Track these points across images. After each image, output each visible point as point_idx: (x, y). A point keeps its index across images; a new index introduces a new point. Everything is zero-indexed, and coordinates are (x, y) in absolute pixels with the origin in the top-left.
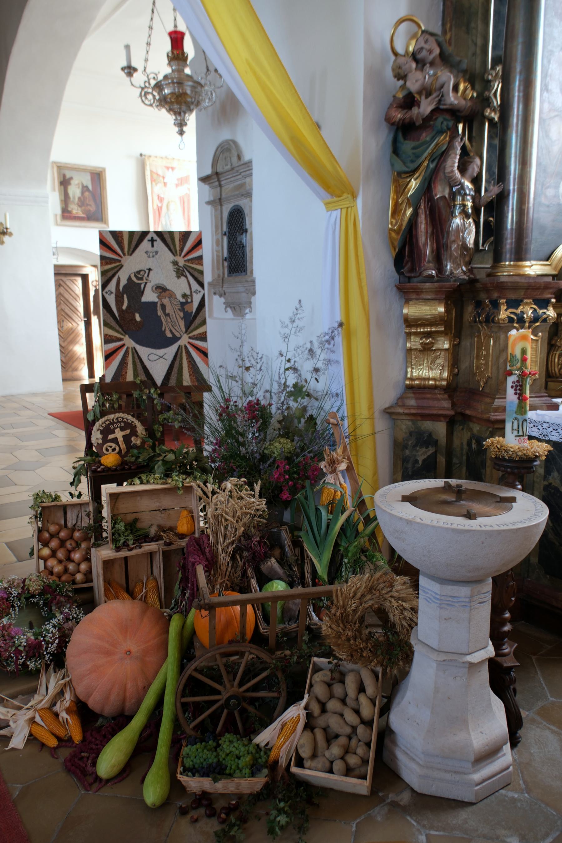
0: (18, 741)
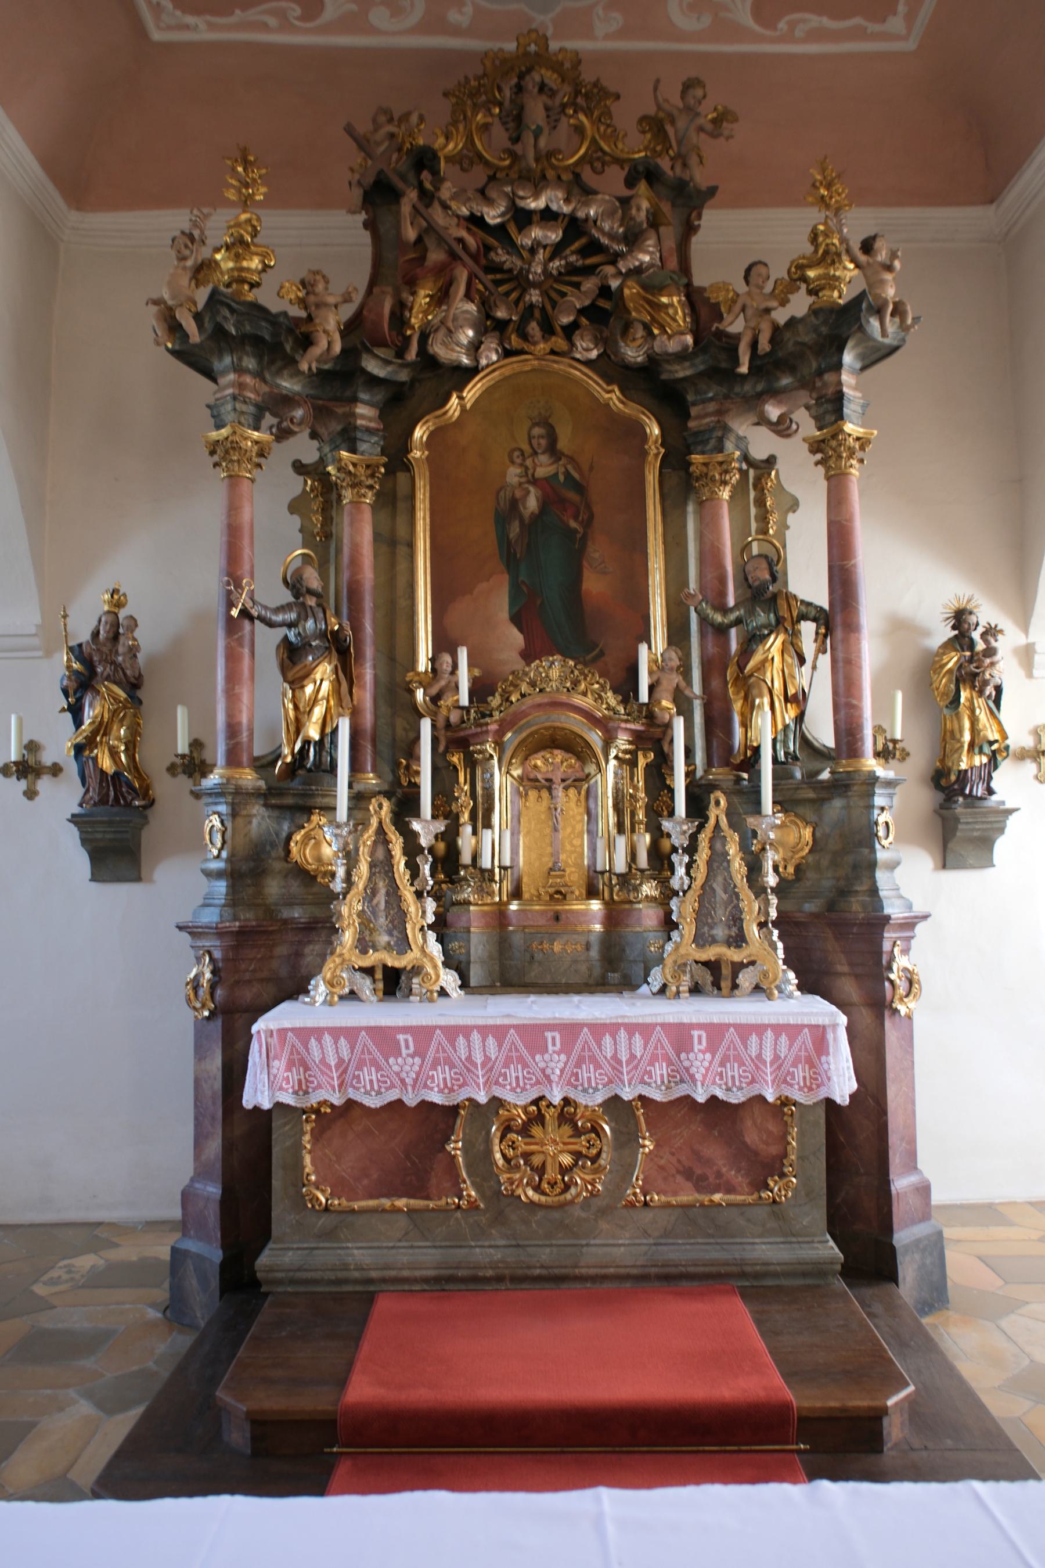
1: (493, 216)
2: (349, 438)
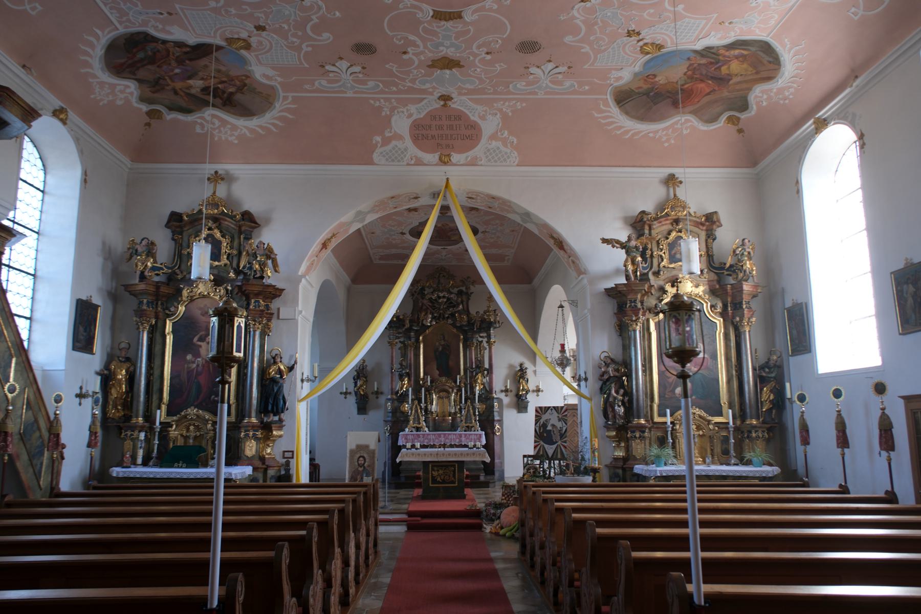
0: (488, 530)
1: (433, 298)
2: (410, 338)
